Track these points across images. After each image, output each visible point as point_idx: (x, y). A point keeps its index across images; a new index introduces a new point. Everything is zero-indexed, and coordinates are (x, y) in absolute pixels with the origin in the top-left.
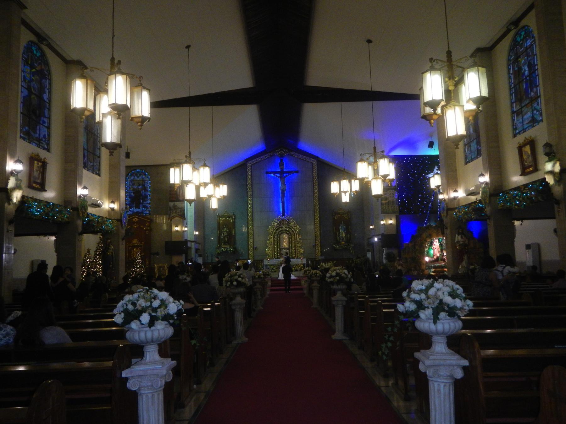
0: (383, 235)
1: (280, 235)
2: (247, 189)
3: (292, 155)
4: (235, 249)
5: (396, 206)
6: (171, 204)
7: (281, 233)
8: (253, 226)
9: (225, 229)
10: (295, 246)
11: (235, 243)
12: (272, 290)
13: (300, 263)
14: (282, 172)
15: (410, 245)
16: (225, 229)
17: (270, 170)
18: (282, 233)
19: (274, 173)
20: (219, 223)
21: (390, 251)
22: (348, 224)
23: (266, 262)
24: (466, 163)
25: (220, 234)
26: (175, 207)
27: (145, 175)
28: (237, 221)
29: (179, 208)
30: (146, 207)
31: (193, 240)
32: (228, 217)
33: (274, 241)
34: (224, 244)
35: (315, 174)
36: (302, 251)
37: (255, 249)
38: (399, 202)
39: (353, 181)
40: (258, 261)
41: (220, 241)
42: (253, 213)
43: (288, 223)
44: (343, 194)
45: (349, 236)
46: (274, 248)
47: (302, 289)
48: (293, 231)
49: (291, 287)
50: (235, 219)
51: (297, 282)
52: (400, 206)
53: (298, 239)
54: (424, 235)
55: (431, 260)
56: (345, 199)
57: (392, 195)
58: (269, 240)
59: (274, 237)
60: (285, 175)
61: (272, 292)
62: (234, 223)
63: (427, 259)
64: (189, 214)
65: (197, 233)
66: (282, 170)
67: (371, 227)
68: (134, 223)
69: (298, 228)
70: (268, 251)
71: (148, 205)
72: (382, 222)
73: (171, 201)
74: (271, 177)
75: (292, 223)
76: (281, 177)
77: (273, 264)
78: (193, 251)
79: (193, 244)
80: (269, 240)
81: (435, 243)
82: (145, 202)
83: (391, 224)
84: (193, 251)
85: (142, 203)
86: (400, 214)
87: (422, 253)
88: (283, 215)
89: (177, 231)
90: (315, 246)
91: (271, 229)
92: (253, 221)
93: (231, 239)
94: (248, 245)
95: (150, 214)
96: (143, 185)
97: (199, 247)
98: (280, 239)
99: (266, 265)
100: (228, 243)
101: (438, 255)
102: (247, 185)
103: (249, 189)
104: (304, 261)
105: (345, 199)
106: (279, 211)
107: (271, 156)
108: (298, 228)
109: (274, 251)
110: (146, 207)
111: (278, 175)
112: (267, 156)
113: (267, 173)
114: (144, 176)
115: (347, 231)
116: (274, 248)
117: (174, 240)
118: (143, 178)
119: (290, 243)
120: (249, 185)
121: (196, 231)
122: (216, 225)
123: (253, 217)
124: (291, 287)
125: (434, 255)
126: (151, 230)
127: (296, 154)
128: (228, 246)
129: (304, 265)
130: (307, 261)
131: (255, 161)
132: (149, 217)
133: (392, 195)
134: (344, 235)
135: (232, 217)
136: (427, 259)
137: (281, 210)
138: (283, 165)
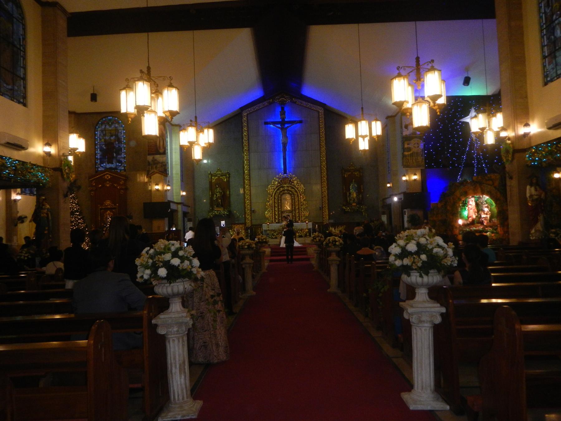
0: (405, 194)
1: (281, 195)
2: (243, 143)
3: (295, 102)
4: (230, 212)
5: (420, 159)
6: (150, 158)
7: (283, 193)
9: (218, 190)
10: (299, 208)
11: (230, 205)
12: (271, 261)
13: (305, 228)
14: (283, 123)
15: (440, 205)
16: (218, 190)
17: (268, 120)
18: (284, 194)
19: (274, 123)
20: (211, 183)
21: (414, 212)
22: (360, 182)
23: (265, 227)
24: (546, 84)
25: (213, 195)
26: (155, 162)
27: (119, 123)
28: (232, 179)
29: (158, 163)
30: (120, 162)
31: (180, 201)
32: (222, 176)
33: (275, 202)
34: (217, 206)
35: (322, 125)
36: (307, 214)
37: (253, 212)
38: (425, 153)
39: (373, 123)
40: (256, 225)
41: (212, 203)
42: (249, 170)
43: (291, 182)
44: (360, 139)
45: (361, 196)
46: (275, 210)
47: (308, 259)
49: (294, 257)
50: (229, 177)
51: (302, 250)
52: (426, 159)
53: (302, 200)
54: (458, 193)
55: (466, 222)
56: (364, 145)
57: (416, 145)
58: (269, 202)
60: (286, 126)
61: (273, 263)
62: (228, 182)
63: (460, 222)
64: (174, 172)
65: (184, 193)
66: (283, 119)
67: (388, 185)
68: (106, 180)
70: (267, 214)
71: (123, 160)
72: (404, 178)
73: (149, 154)
74: (270, 128)
75: (295, 182)
76: (281, 128)
77: (274, 229)
78: (180, 215)
79: (180, 206)
80: (269, 202)
81: (471, 203)
82: (119, 156)
83: (415, 180)
84: (180, 215)
85: (116, 157)
86: (426, 167)
87: (456, 214)
88: (285, 172)
89: (158, 190)
90: (321, 209)
91: (271, 189)
92: (250, 180)
93: (225, 201)
94: (245, 208)
95: (125, 170)
96: (117, 136)
97: (189, 210)
98: (281, 201)
99: (266, 231)
100: (222, 206)
101: (474, 217)
102: (242, 138)
103: (245, 143)
104: (310, 225)
105: (364, 145)
106: (281, 168)
107: (270, 104)
108: (302, 188)
109: (275, 214)
110: (120, 162)
111: (279, 126)
112: (266, 103)
113: (266, 123)
114: (117, 125)
115: (359, 191)
116: (275, 210)
117: (154, 200)
118: (116, 127)
119: (293, 205)
120: (245, 138)
121: (183, 191)
122: (208, 186)
123: (250, 175)
124: (294, 257)
125: (468, 217)
126: (126, 189)
127: (299, 101)
128: (221, 209)
129: (309, 229)
130: (314, 225)
131: (251, 109)
132: (124, 173)
133: (416, 145)
134: (355, 195)
135: (225, 175)
136: (460, 222)
137: (282, 167)
138: (284, 114)
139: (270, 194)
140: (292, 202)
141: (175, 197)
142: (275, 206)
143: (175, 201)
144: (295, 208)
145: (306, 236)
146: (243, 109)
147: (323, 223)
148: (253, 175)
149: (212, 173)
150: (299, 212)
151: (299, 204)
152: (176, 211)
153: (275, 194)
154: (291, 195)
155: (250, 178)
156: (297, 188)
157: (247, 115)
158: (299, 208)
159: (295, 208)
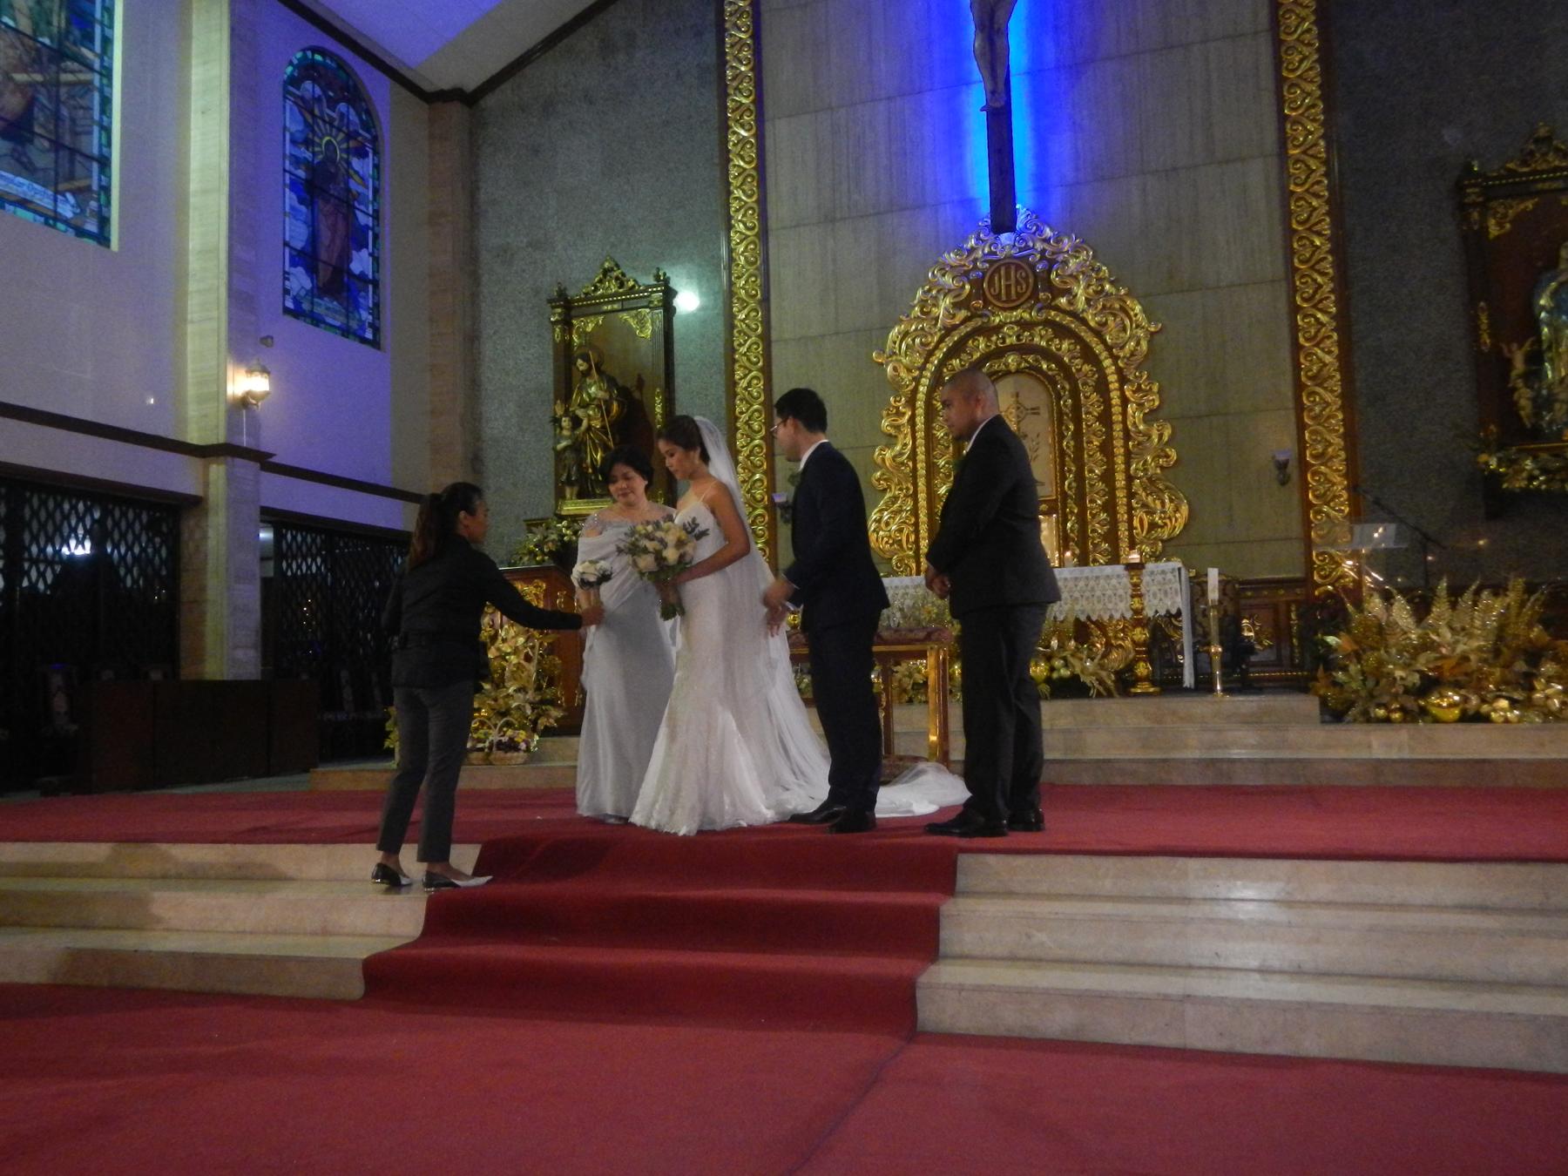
8: (766, 339)
13: (1121, 608)
31: (219, 437)
48: (1089, 355)
75: (1080, 291)
79: (217, 471)
80: (890, 440)
88: (1002, 219)
92: (765, 302)
106: (967, 203)
137: (980, 186)
141: (192, 411)
143: (194, 437)
144: (1080, 477)
145: (1125, 683)
147: (1306, 582)
148: (783, 275)
149: (572, 293)
150: (1110, 507)
151: (1106, 449)
152: (195, 504)
155: (766, 289)
156: (1098, 334)
158: (1108, 477)
159: (1080, 477)
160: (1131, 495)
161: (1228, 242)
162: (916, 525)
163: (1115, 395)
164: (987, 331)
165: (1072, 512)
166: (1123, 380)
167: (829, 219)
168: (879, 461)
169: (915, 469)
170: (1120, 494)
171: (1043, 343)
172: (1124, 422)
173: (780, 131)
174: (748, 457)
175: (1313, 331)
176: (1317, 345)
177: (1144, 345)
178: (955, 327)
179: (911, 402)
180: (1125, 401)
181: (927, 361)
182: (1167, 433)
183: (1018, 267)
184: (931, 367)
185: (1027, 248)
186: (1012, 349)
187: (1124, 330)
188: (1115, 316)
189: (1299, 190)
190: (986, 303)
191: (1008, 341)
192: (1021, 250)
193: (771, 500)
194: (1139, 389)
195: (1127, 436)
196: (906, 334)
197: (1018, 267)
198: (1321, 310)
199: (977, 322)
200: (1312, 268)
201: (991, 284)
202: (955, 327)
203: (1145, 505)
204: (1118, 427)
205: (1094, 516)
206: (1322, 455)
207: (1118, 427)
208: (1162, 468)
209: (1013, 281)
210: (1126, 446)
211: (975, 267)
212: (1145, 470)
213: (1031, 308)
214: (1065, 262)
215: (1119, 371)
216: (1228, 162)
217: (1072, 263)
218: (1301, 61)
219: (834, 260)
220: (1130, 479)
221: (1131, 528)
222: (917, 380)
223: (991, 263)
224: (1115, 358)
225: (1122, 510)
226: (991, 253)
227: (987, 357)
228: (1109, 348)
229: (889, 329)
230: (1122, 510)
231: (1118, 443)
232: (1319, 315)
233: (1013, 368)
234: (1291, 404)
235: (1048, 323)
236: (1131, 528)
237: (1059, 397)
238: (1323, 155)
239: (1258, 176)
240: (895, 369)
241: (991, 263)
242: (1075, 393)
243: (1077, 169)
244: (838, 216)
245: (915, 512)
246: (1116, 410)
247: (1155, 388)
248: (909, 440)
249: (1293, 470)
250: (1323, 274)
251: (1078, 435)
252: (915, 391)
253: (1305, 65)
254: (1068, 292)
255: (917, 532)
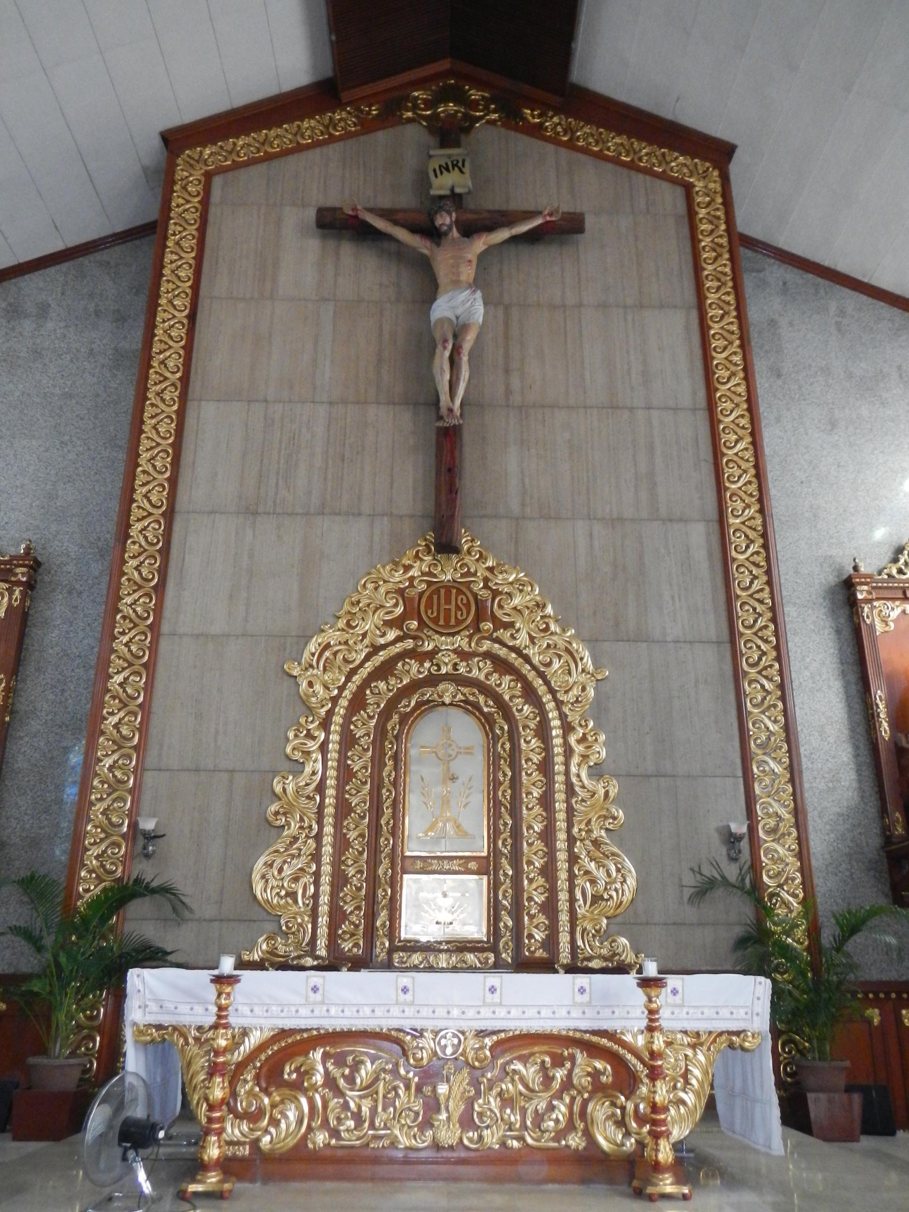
10: (548, 836)
33: (346, 774)
46: (342, 844)
48: (530, 694)
53: (580, 772)
59: (348, 741)
69: (577, 676)
80: (297, 768)
107: (367, 126)
127: (553, 122)
139: (310, 710)
140: (494, 784)
142: (343, 809)
146: (176, 140)
150: (549, 871)
151: (546, 801)
153: (358, 703)
154: (487, 722)
156: (541, 675)
157: (208, 176)
158: (548, 836)
159: (516, 834)
160: (573, 859)
161: (673, 598)
162: (317, 875)
163: (558, 741)
164: (421, 657)
165: (506, 875)
166: (567, 728)
167: (251, 511)
168: (278, 789)
169: (321, 807)
170: (562, 856)
171: (482, 677)
172: (567, 773)
173: (207, 416)
174: (111, 768)
175: (760, 698)
176: (763, 712)
177: (591, 692)
178: (384, 647)
179: (325, 724)
180: (568, 752)
181: (349, 678)
182: (613, 792)
183: (460, 592)
184: (352, 687)
185: (468, 574)
186: (447, 677)
187: (570, 674)
188: (560, 657)
189: (741, 557)
190: (421, 622)
191: (444, 671)
192: (463, 576)
193: (133, 826)
194: (583, 740)
195: (570, 791)
196: (328, 646)
197: (460, 592)
198: (766, 677)
199: (409, 644)
200: (756, 634)
201: (429, 605)
202: (384, 647)
203: (587, 873)
204: (560, 778)
205: (531, 881)
206: (774, 831)
207: (560, 778)
208: (607, 830)
209: (453, 607)
210: (568, 801)
211: (411, 585)
212: (589, 831)
213: (470, 637)
214: (510, 595)
215: (562, 717)
216: (671, 520)
217: (517, 601)
218: (737, 442)
219: (251, 556)
220: (571, 840)
221: (572, 900)
222: (335, 700)
223: (429, 584)
224: (559, 704)
225: (563, 875)
226: (430, 574)
227: (415, 686)
228: (552, 691)
229: (307, 639)
230: (563, 875)
231: (560, 796)
232: (765, 682)
233: (447, 700)
234: (740, 773)
235: (488, 655)
236: (572, 900)
237: (496, 739)
238: (760, 528)
239: (698, 537)
240: (311, 684)
241: (429, 584)
242: (513, 736)
243: (523, 505)
244: (261, 509)
245: (316, 857)
246: (559, 759)
247: (602, 738)
248: (319, 766)
249: (744, 845)
250: (766, 641)
251: (515, 783)
252: (330, 713)
253: (740, 446)
254: (511, 625)
255: (317, 884)
